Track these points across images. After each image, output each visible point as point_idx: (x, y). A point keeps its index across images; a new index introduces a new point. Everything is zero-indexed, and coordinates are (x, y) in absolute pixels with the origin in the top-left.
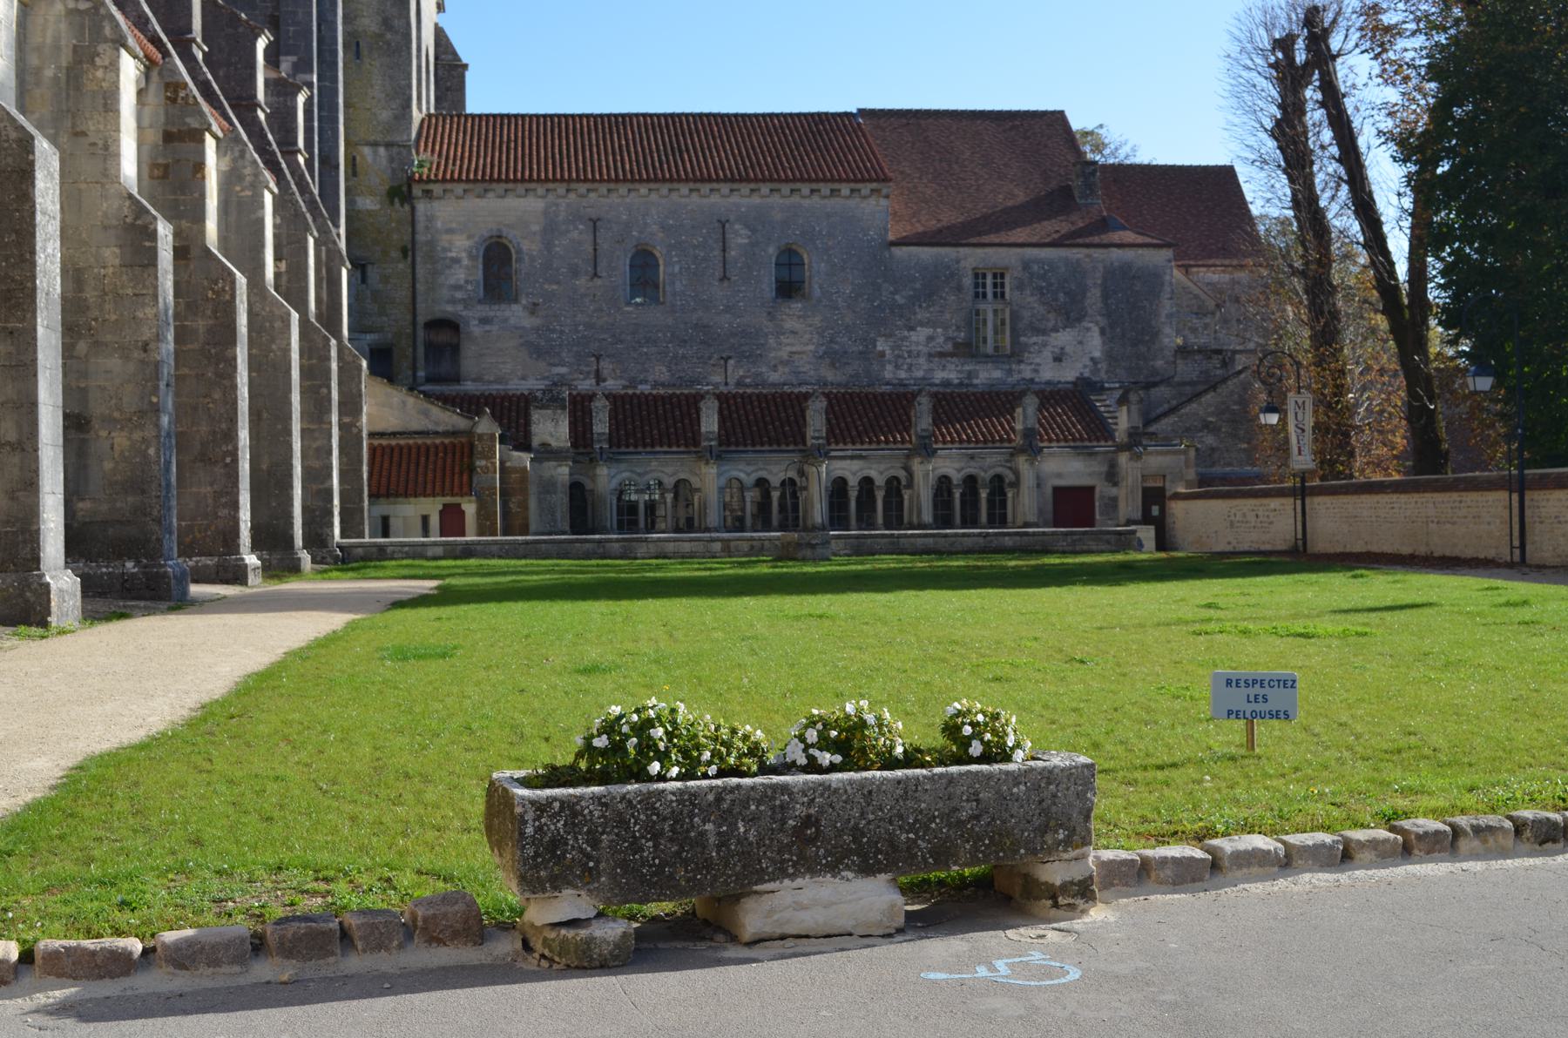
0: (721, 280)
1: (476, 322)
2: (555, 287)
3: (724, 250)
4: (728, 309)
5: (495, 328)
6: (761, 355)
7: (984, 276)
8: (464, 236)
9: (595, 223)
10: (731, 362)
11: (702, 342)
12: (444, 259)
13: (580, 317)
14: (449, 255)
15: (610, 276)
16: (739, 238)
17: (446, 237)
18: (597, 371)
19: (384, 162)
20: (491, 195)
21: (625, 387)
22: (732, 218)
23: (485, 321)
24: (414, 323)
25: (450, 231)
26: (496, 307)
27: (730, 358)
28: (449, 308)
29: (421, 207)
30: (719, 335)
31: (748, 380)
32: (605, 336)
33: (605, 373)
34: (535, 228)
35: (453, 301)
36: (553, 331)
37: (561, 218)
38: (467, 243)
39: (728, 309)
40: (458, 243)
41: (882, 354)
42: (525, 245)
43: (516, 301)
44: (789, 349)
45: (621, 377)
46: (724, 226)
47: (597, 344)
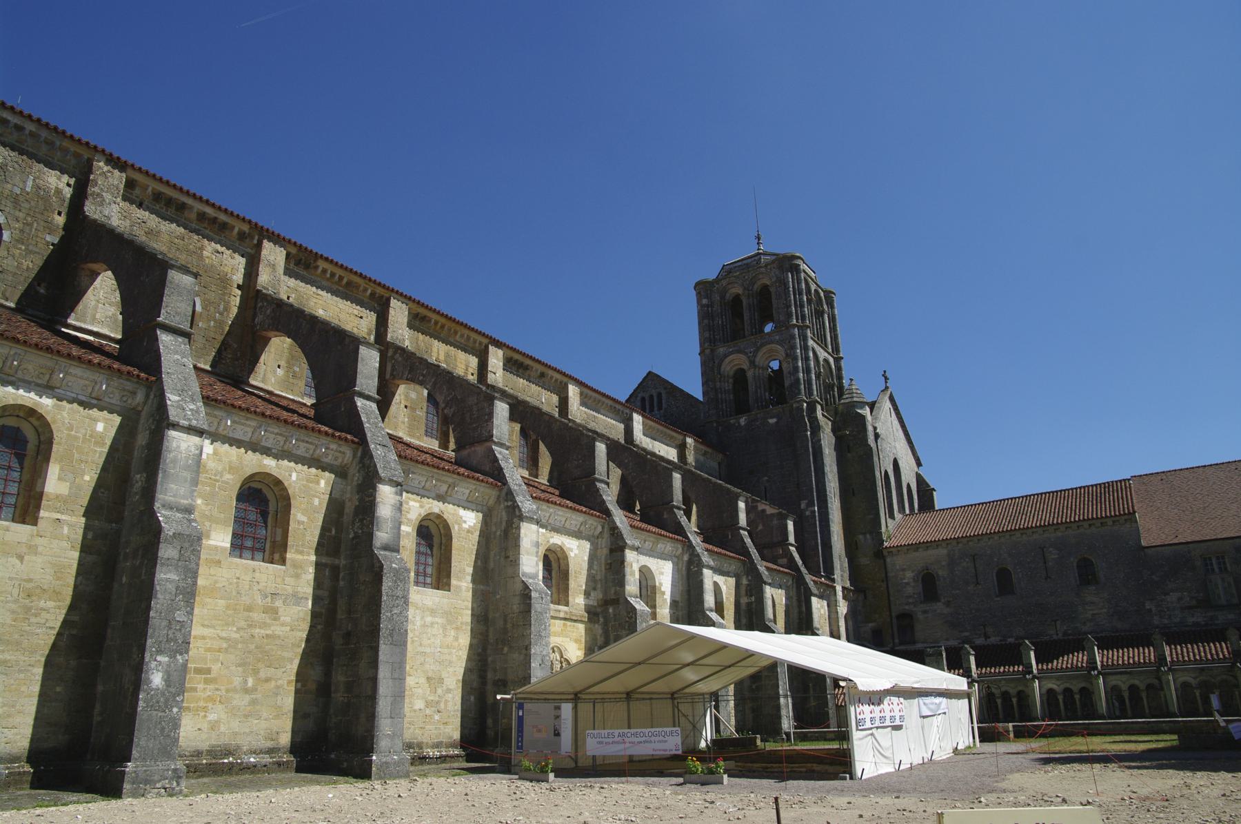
0: (1046, 579)
7: (1210, 559)
9: (974, 558)
10: (1058, 622)
16: (1053, 555)
18: (985, 633)
20: (920, 550)
21: (1001, 641)
24: (891, 615)
28: (907, 607)
29: (888, 560)
31: (1070, 632)
35: (908, 604)
41: (1150, 610)
42: (940, 573)
43: (939, 601)
44: (1091, 612)
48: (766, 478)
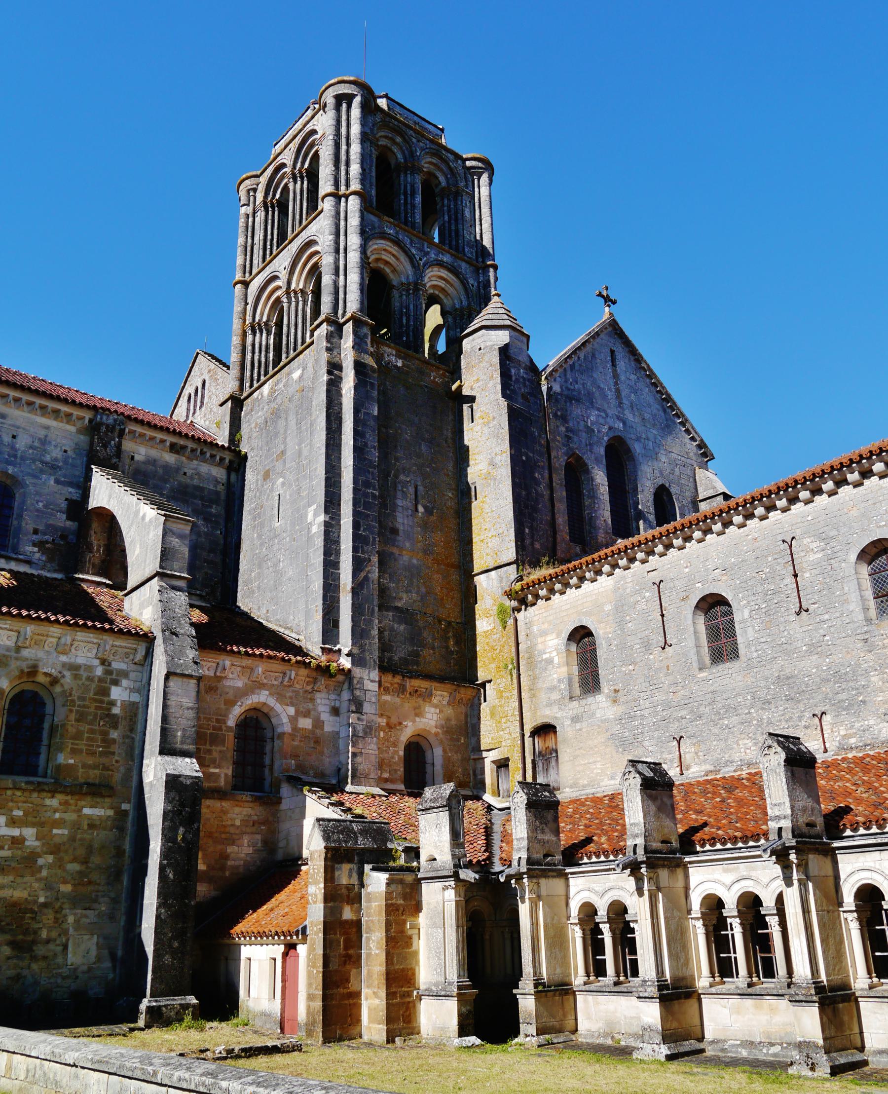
1: (569, 722)
2: (631, 668)
3: (796, 576)
4: (813, 648)
5: (584, 724)
6: (864, 702)
8: (554, 636)
10: (826, 719)
11: (789, 699)
12: (541, 661)
13: (659, 697)
14: (545, 656)
15: (680, 641)
17: (540, 640)
19: (496, 583)
22: (798, 533)
23: (576, 719)
25: (544, 633)
26: (584, 701)
27: (823, 713)
30: (807, 685)
31: (853, 741)
32: (683, 713)
33: (687, 758)
34: (608, 608)
35: (549, 705)
36: (632, 718)
37: (628, 591)
38: (556, 641)
39: (813, 648)
40: (550, 643)
45: (705, 761)
46: (791, 546)
47: (677, 724)
48: (281, 480)
